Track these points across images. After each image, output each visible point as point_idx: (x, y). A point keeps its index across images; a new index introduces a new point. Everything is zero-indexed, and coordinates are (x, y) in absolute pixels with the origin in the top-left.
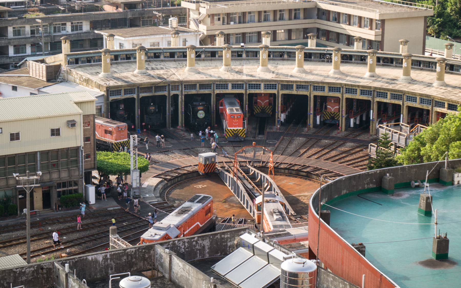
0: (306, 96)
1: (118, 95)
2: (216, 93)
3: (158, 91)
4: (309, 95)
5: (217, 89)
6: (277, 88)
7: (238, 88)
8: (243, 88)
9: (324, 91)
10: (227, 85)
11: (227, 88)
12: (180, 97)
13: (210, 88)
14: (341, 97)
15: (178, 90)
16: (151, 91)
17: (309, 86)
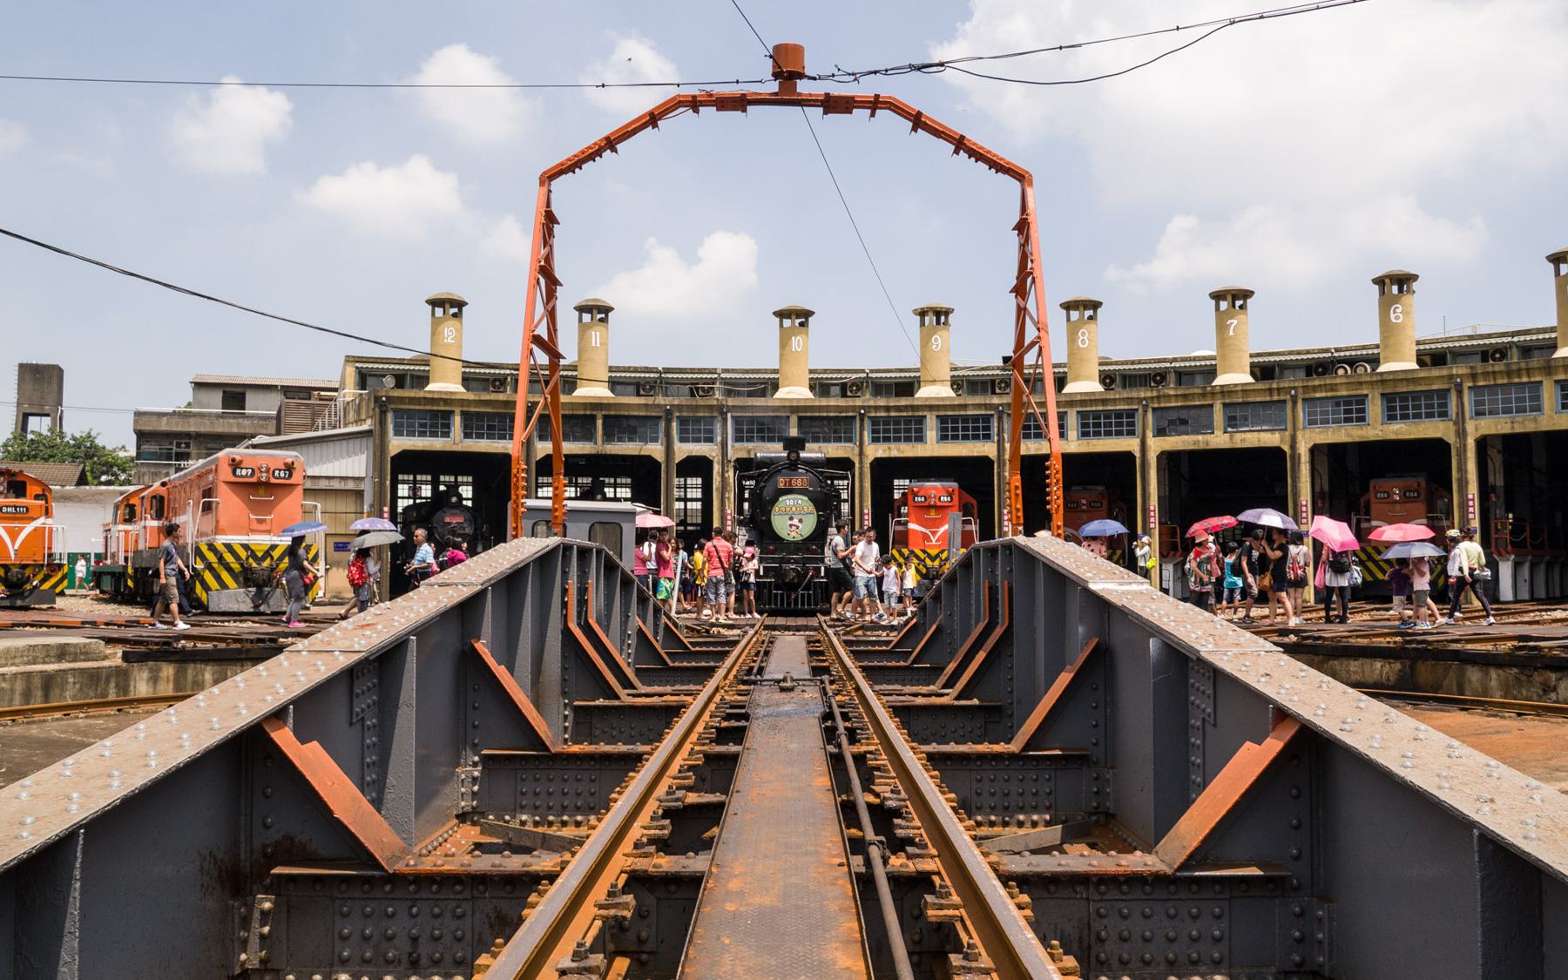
0: (1275, 454)
1: (434, 434)
2: (871, 459)
3: (620, 440)
4: (1286, 448)
5: (875, 440)
6: (1138, 428)
7: (965, 437)
8: (987, 437)
9: (1362, 419)
10: (921, 420)
11: (920, 439)
12: (717, 468)
13: (849, 440)
14: (1451, 439)
15: (710, 440)
16: (589, 436)
17: (1289, 405)
